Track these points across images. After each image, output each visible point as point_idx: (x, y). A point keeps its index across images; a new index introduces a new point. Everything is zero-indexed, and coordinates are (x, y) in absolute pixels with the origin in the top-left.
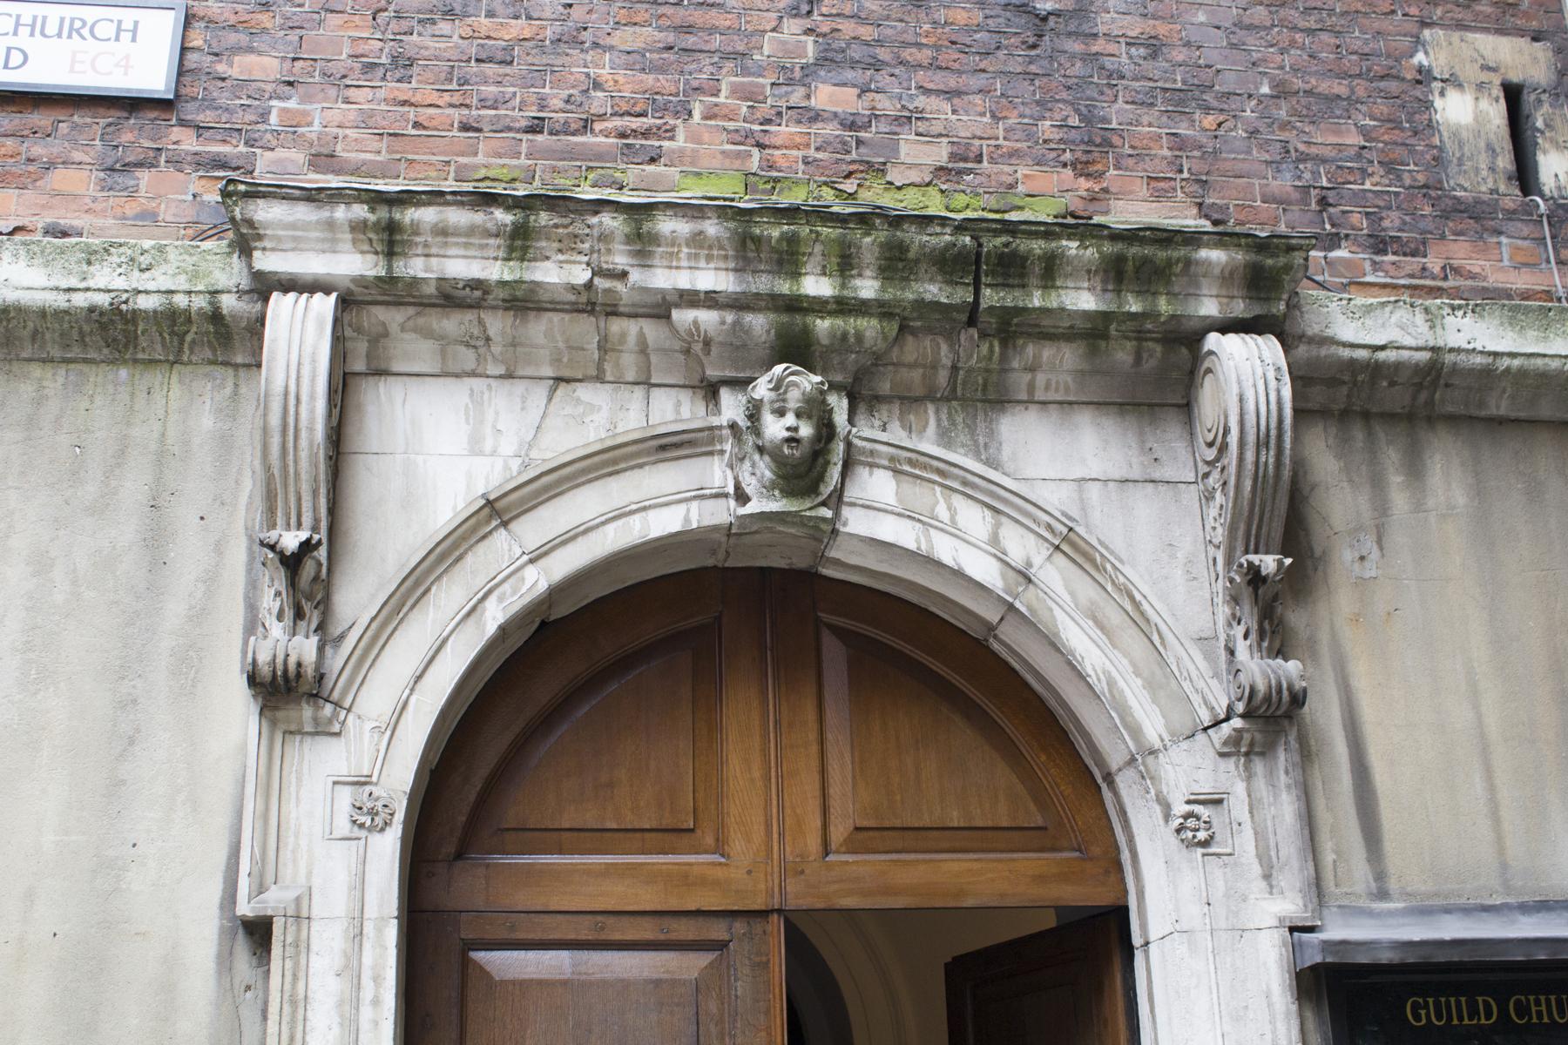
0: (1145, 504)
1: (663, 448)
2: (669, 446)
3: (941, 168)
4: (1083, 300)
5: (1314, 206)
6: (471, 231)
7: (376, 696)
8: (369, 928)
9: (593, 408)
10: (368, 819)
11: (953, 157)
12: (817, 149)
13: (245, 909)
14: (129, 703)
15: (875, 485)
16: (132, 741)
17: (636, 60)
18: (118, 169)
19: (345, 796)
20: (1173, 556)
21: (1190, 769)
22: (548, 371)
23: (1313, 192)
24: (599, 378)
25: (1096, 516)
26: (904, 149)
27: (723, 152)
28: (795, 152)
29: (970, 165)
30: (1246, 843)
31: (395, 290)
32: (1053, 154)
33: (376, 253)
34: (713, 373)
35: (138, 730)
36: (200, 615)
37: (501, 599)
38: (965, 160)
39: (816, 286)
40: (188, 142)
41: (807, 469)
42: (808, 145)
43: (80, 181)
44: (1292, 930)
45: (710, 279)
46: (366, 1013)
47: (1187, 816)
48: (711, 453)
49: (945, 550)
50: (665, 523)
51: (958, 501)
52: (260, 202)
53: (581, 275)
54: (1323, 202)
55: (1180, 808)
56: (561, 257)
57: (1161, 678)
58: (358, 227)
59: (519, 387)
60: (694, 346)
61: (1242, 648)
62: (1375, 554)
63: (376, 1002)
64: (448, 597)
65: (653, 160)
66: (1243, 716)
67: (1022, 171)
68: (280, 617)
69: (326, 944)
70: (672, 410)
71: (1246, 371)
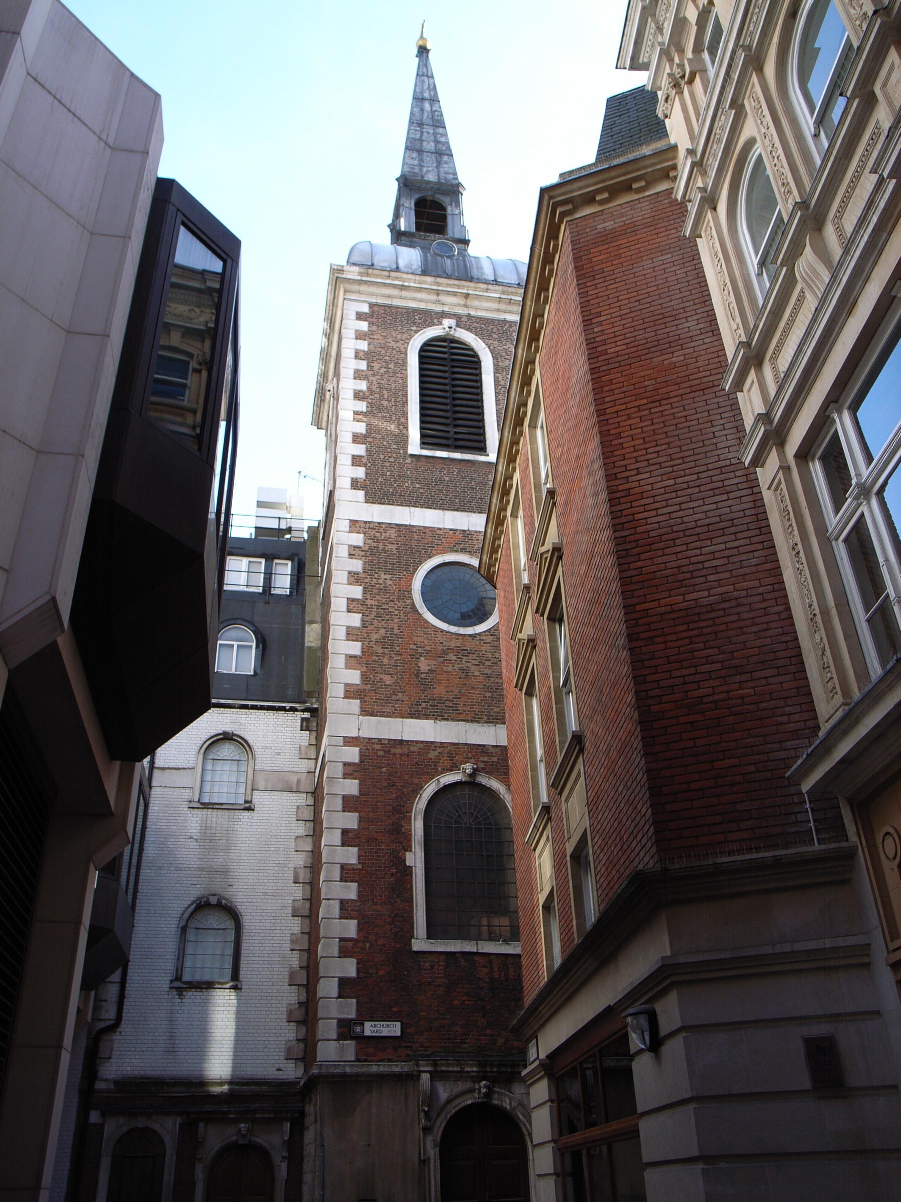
2: (471, 1091)
7: (436, 1130)
10: (435, 1146)
15: (496, 1096)
31: (436, 1071)
39: (488, 1070)
50: (469, 1102)
60: (472, 1077)
64: (444, 1115)
69: (432, 1162)
70: (468, 1085)
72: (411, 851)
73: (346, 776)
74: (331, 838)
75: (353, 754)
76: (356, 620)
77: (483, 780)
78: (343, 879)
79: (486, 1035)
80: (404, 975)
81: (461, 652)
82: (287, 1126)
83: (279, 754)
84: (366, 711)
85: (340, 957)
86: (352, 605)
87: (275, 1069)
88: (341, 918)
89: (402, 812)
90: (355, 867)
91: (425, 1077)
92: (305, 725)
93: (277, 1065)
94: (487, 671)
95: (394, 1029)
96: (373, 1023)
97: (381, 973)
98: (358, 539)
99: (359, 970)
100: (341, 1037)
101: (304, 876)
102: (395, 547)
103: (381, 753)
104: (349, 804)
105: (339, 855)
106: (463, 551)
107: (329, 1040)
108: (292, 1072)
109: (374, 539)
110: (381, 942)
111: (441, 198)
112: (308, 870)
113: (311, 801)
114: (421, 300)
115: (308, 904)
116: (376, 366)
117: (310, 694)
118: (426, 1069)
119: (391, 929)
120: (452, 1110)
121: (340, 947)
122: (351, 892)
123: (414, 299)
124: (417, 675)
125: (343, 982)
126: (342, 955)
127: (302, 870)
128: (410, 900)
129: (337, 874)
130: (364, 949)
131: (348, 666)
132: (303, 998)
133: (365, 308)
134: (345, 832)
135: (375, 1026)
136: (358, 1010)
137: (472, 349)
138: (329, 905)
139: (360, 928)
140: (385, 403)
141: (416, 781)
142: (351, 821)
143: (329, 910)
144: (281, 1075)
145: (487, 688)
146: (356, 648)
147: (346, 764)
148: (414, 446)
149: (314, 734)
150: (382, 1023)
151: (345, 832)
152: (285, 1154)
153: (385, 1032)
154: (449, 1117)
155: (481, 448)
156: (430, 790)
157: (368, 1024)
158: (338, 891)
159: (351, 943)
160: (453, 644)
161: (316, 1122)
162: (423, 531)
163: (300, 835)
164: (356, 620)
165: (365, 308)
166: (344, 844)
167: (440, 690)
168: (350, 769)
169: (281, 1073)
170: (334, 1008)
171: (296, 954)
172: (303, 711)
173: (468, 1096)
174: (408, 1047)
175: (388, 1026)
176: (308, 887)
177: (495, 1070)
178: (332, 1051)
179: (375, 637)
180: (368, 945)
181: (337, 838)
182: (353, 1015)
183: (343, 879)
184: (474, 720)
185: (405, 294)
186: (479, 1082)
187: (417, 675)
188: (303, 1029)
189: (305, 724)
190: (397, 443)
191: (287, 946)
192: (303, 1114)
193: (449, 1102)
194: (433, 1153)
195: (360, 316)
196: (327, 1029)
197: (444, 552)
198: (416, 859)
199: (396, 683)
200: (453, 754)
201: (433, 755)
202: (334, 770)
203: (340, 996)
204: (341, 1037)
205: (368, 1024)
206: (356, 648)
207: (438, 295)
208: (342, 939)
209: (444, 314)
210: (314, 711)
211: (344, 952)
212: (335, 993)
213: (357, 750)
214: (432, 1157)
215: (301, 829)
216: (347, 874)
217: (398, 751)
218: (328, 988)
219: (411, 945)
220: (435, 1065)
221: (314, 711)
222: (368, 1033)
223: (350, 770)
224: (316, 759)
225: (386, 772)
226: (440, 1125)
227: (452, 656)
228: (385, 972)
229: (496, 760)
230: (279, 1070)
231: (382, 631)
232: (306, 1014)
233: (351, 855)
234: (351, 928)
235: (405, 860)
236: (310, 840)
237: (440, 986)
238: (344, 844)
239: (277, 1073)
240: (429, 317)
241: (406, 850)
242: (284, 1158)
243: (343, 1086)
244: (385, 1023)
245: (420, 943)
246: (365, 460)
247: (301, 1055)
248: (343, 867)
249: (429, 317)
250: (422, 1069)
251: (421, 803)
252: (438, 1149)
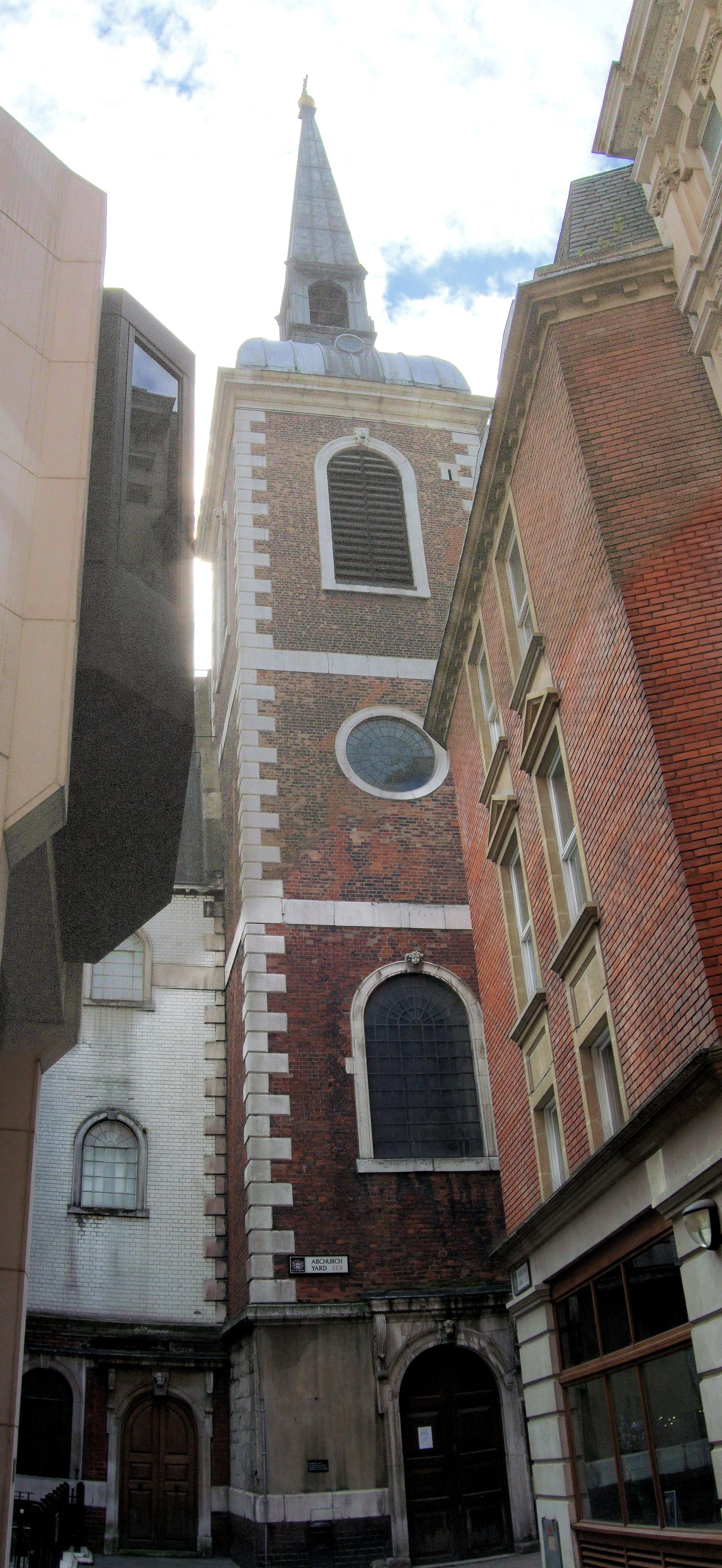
2: (432, 1332)
10: (393, 1396)
13: (380, 1412)
17: (419, 1259)
18: (343, 1288)
30: (516, 1389)
40: (353, 1282)
41: (453, 1336)
43: (337, 1290)
49: (472, 1345)
50: (431, 1345)
57: (503, 1365)
60: (433, 1316)
69: (391, 1416)
72: (351, 1056)
73: (271, 969)
74: (254, 1044)
75: (277, 944)
76: (271, 787)
77: (429, 969)
78: (273, 1091)
79: (448, 1267)
80: (350, 1202)
81: (399, 821)
82: (210, 1379)
83: (180, 944)
84: (290, 894)
85: (272, 1182)
86: (266, 771)
87: (192, 1312)
88: (271, 1136)
89: (337, 1011)
90: (286, 1077)
91: (380, 1319)
92: (210, 911)
93: (195, 1308)
94: (431, 842)
95: (340, 1265)
96: (315, 1258)
97: (322, 1200)
98: (269, 692)
99: (295, 1198)
100: (278, 1275)
101: (218, 1088)
102: (312, 700)
103: (310, 942)
104: (275, 1002)
105: (264, 1062)
106: (392, 702)
107: (264, 1279)
108: (213, 1315)
109: (286, 691)
110: (319, 1164)
111: (345, 285)
112: (221, 1081)
113: (220, 1000)
114: (326, 406)
115: (222, 1121)
116: (278, 486)
117: (212, 875)
118: (380, 1310)
119: (332, 1147)
121: (272, 1171)
122: (282, 1105)
123: (316, 405)
124: (349, 850)
125: (278, 1212)
126: (275, 1179)
127: (215, 1081)
128: (353, 1114)
129: (265, 1085)
130: (300, 1172)
131: (264, 842)
132: (222, 1230)
133: (261, 418)
134: (272, 1036)
135: (318, 1262)
136: (297, 1244)
137: (390, 463)
138: (257, 1122)
139: (295, 1149)
140: (291, 530)
141: (352, 974)
142: (279, 1022)
143: (256, 1128)
144: (200, 1319)
145: (432, 863)
146: (273, 821)
147: (269, 956)
148: (328, 580)
149: (221, 921)
150: (325, 1258)
151: (272, 1036)
152: (209, 1409)
153: (330, 1269)
154: (408, 1363)
155: (408, 581)
156: (370, 983)
157: (309, 1260)
158: (265, 1105)
159: (284, 1166)
160: (389, 811)
161: (252, 1372)
162: (345, 680)
163: (210, 1040)
164: (271, 787)
165: (261, 418)
166: (271, 1050)
167: (376, 867)
168: (275, 962)
169: (199, 1316)
170: (268, 1241)
171: (211, 1180)
172: (206, 894)
173: (430, 1338)
174: (357, 1285)
175: (332, 1261)
176: (222, 1102)
178: (266, 1290)
179: (294, 807)
180: (304, 1167)
181: (263, 1042)
182: (291, 1249)
183: (273, 1091)
184: (419, 900)
185: (307, 399)
186: (442, 1321)
187: (349, 850)
188: (224, 1266)
189: (208, 909)
190: (307, 577)
191: (201, 1170)
192: (228, 1365)
194: (392, 1406)
195: (255, 427)
196: (261, 1266)
197: (369, 705)
198: (356, 1065)
199: (324, 859)
200: (397, 940)
201: (371, 942)
202: (255, 963)
203: (275, 1228)
204: (278, 1275)
205: (309, 1260)
206: (273, 821)
207: (347, 399)
208: (274, 1162)
209: (355, 422)
210: (218, 895)
211: (277, 1177)
212: (269, 1224)
213: (281, 939)
214: (391, 1411)
215: (212, 1034)
216: (277, 1084)
217: (330, 939)
218: (259, 1219)
219: (355, 1166)
220: (390, 1303)
221: (218, 895)
222: (309, 1269)
223: (275, 963)
224: (226, 952)
225: (316, 966)
226: (397, 1375)
227: (388, 826)
228: (327, 1201)
229: (458, 948)
230: (197, 1313)
231: (303, 801)
232: (230, 1249)
233: (280, 1063)
234: (284, 1148)
235: (344, 1068)
236: (221, 1046)
237: (391, 1213)
238: (271, 1050)
239: (195, 1316)
240: (336, 426)
241: (345, 1055)
242: (208, 1413)
243: (287, 1331)
244: (329, 1258)
245: (366, 1164)
246: (271, 599)
247: (222, 1296)
248: (272, 1077)
249: (336, 426)
250: (375, 1309)
251: (360, 1000)
252: (397, 1401)
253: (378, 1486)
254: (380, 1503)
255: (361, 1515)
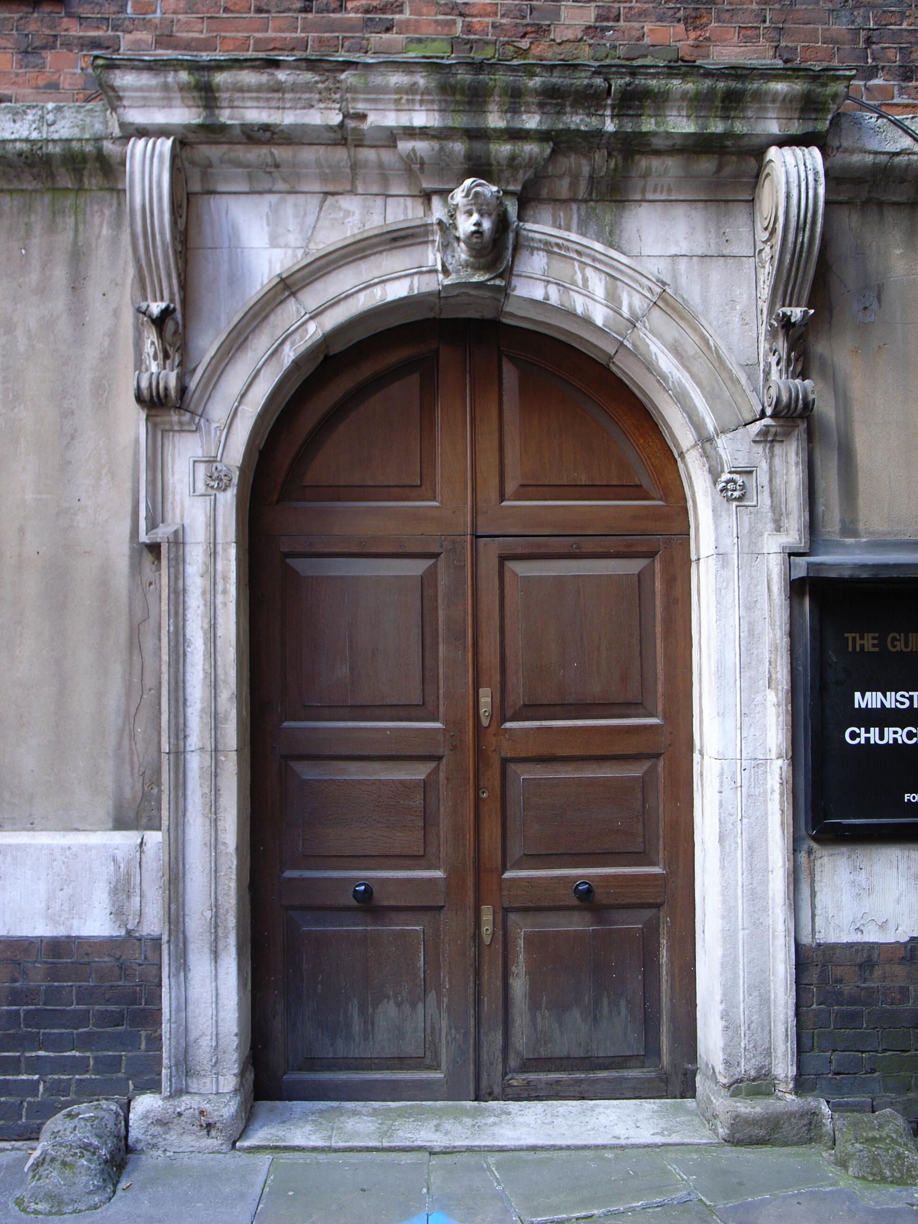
0: (717, 274)
1: (395, 240)
2: (400, 238)
3: (590, 27)
4: (681, 124)
5: (862, 45)
6: (259, 88)
8: (219, 548)
9: (348, 213)
10: (217, 482)
11: (599, 18)
12: (503, 16)
13: (144, 538)
14: (67, 414)
15: (536, 263)
16: (73, 438)
19: (201, 469)
20: (733, 309)
21: (734, 449)
22: (317, 187)
23: (862, 33)
24: (353, 192)
25: (683, 281)
26: (563, 13)
27: (436, 21)
28: (487, 19)
29: (611, 24)
30: (765, 500)
31: (212, 131)
32: (671, 12)
33: (198, 107)
34: (427, 185)
35: (76, 430)
36: (108, 357)
37: (293, 344)
38: (608, 20)
39: (495, 120)
40: (76, 31)
42: (496, 14)
44: (790, 555)
45: (420, 119)
46: (220, 598)
47: (727, 482)
48: (426, 242)
49: (579, 304)
50: (397, 290)
51: (589, 272)
52: (117, 72)
53: (335, 118)
54: (869, 41)
55: (725, 476)
56: (322, 105)
58: (183, 88)
59: (301, 198)
60: (412, 168)
61: (774, 369)
62: (875, 306)
63: (225, 592)
64: (261, 344)
65: (388, 30)
66: (771, 417)
67: (647, 27)
68: (155, 358)
69: (196, 556)
70: (401, 212)
71: (794, 173)
118: (159, 117)
120: (305, 326)
177: (532, 122)
193: (287, 287)
194: (205, 518)
214: (197, 536)
226: (241, 397)
250: (137, 116)
252: (228, 499)
253: (120, 824)
254: (122, 889)
255: (38, 927)
